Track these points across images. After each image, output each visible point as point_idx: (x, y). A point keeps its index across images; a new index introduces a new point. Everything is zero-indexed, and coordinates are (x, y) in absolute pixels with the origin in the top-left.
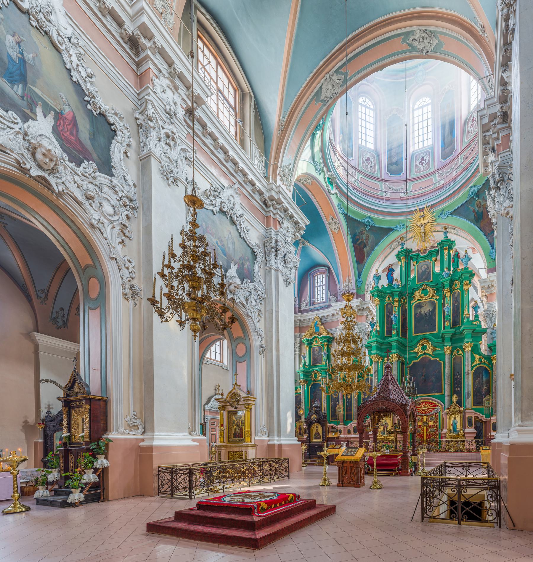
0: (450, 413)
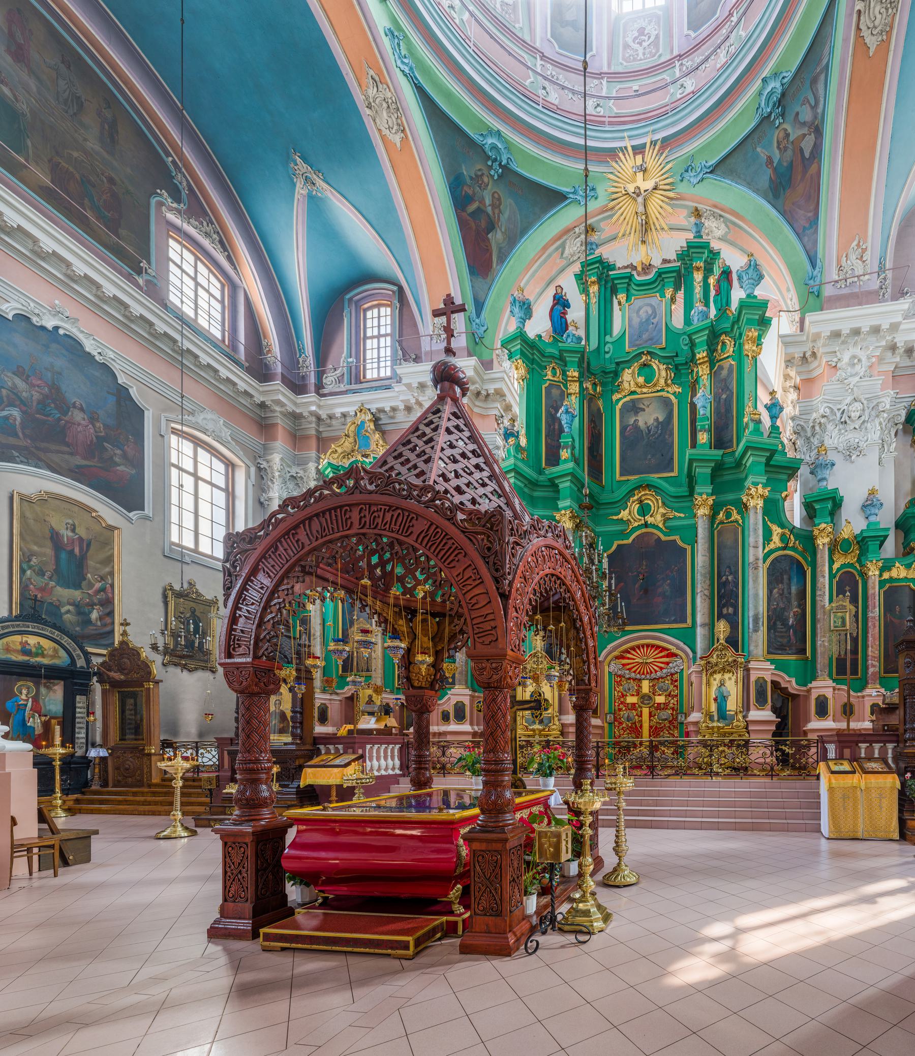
0: (710, 669)
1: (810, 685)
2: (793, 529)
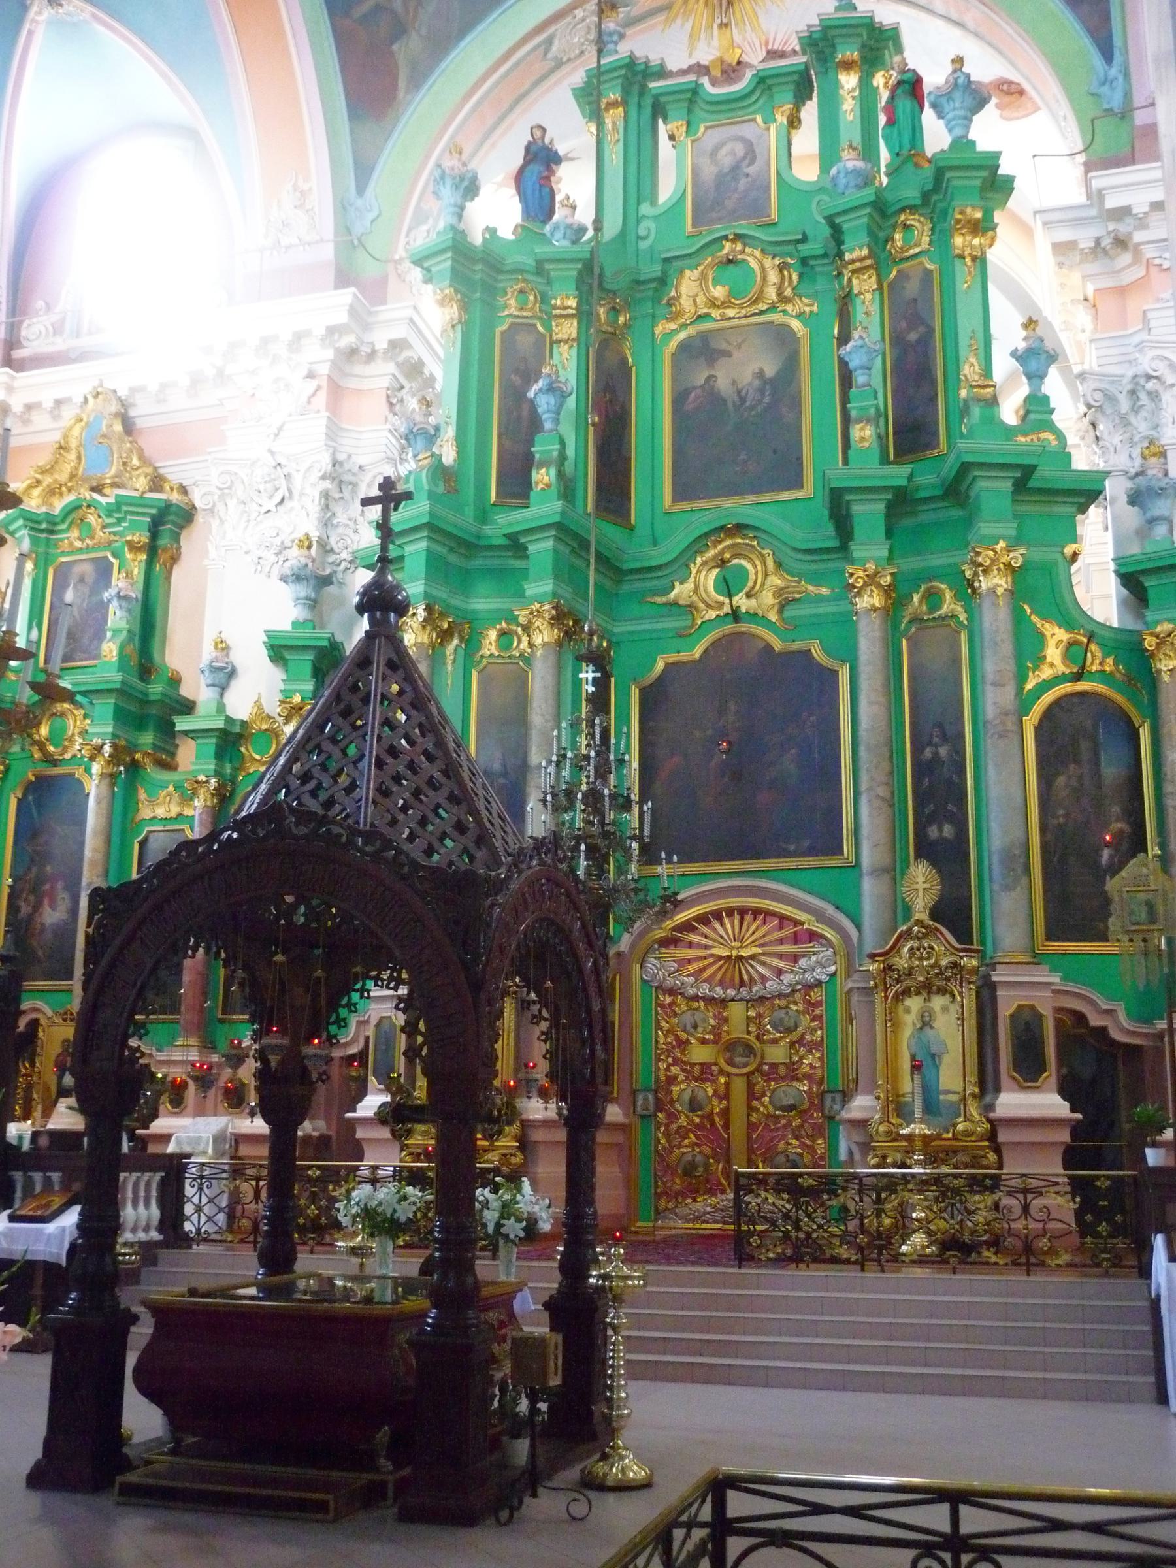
2: (1094, 633)
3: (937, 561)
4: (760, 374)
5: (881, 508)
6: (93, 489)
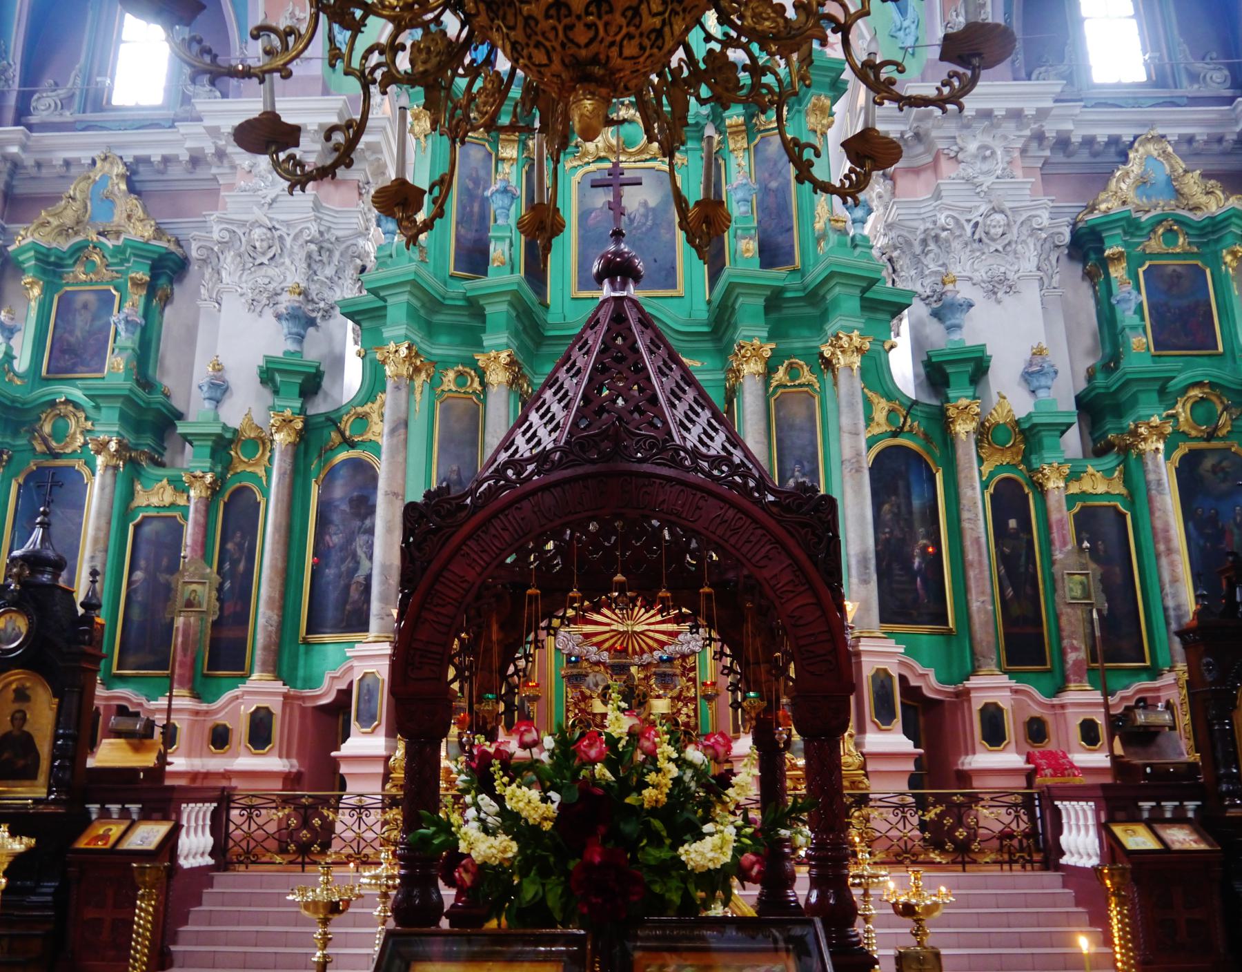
1: (968, 684)
3: (798, 344)
4: (645, 204)
5: (761, 302)
6: (99, 234)
